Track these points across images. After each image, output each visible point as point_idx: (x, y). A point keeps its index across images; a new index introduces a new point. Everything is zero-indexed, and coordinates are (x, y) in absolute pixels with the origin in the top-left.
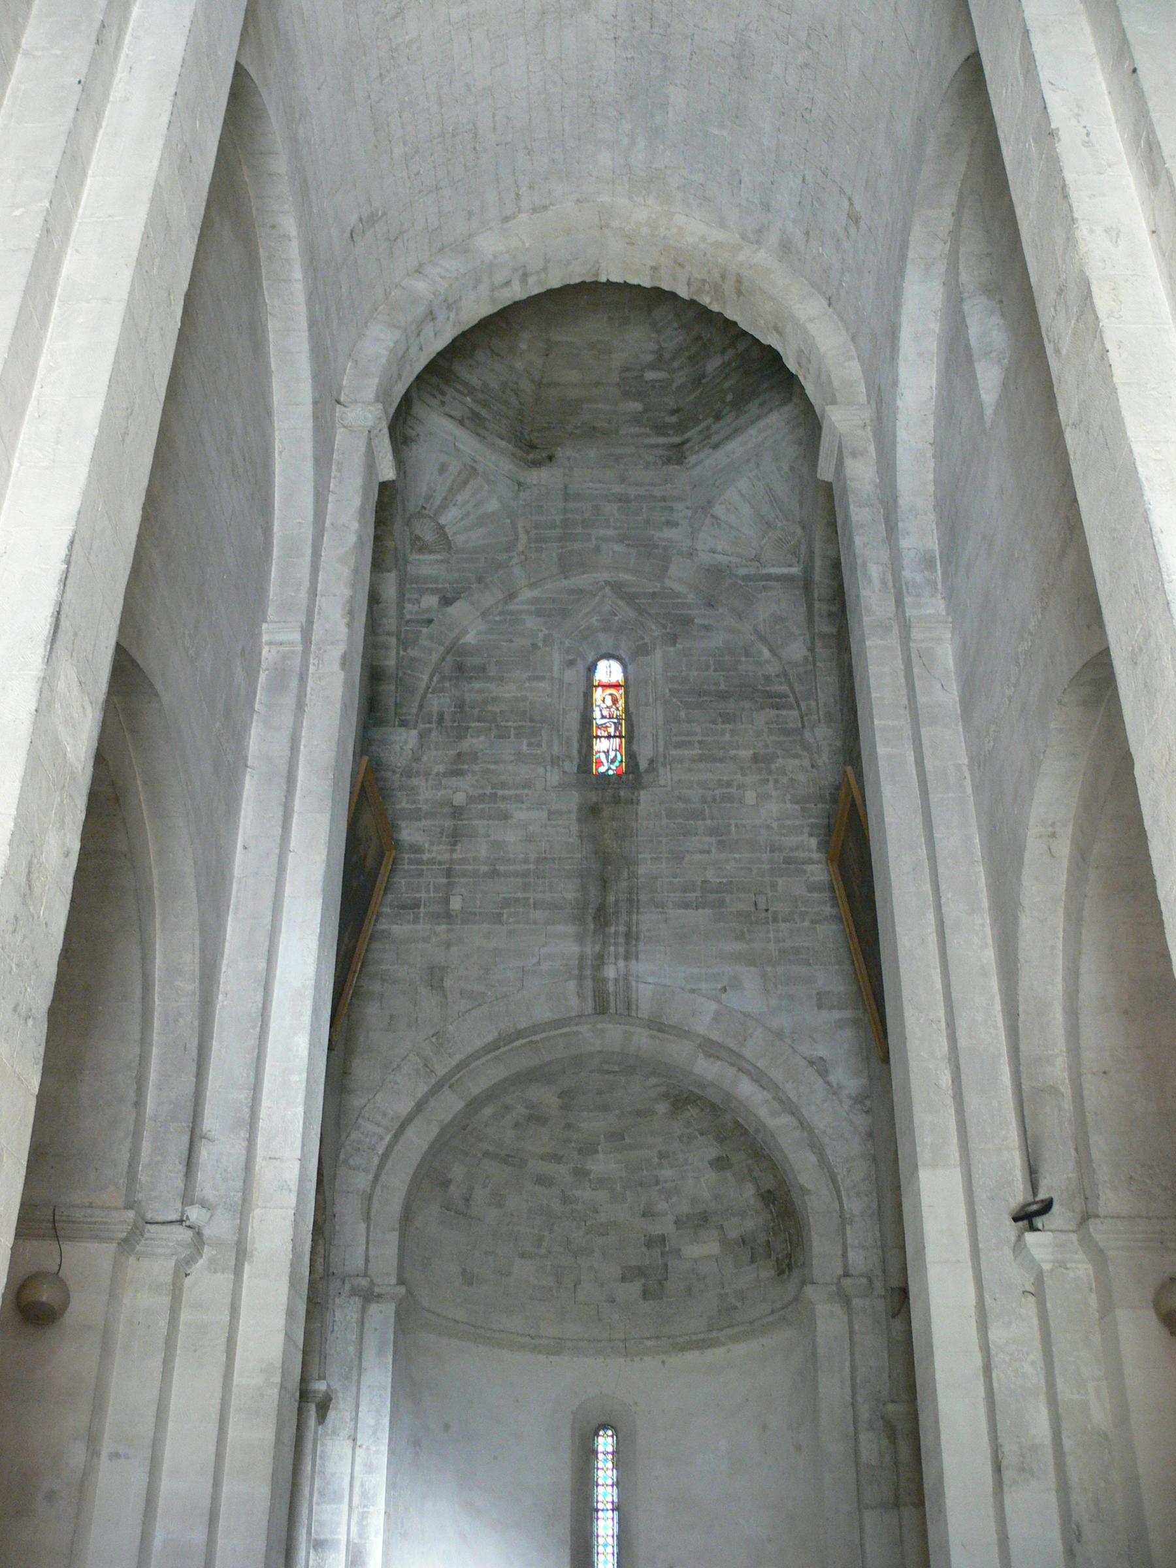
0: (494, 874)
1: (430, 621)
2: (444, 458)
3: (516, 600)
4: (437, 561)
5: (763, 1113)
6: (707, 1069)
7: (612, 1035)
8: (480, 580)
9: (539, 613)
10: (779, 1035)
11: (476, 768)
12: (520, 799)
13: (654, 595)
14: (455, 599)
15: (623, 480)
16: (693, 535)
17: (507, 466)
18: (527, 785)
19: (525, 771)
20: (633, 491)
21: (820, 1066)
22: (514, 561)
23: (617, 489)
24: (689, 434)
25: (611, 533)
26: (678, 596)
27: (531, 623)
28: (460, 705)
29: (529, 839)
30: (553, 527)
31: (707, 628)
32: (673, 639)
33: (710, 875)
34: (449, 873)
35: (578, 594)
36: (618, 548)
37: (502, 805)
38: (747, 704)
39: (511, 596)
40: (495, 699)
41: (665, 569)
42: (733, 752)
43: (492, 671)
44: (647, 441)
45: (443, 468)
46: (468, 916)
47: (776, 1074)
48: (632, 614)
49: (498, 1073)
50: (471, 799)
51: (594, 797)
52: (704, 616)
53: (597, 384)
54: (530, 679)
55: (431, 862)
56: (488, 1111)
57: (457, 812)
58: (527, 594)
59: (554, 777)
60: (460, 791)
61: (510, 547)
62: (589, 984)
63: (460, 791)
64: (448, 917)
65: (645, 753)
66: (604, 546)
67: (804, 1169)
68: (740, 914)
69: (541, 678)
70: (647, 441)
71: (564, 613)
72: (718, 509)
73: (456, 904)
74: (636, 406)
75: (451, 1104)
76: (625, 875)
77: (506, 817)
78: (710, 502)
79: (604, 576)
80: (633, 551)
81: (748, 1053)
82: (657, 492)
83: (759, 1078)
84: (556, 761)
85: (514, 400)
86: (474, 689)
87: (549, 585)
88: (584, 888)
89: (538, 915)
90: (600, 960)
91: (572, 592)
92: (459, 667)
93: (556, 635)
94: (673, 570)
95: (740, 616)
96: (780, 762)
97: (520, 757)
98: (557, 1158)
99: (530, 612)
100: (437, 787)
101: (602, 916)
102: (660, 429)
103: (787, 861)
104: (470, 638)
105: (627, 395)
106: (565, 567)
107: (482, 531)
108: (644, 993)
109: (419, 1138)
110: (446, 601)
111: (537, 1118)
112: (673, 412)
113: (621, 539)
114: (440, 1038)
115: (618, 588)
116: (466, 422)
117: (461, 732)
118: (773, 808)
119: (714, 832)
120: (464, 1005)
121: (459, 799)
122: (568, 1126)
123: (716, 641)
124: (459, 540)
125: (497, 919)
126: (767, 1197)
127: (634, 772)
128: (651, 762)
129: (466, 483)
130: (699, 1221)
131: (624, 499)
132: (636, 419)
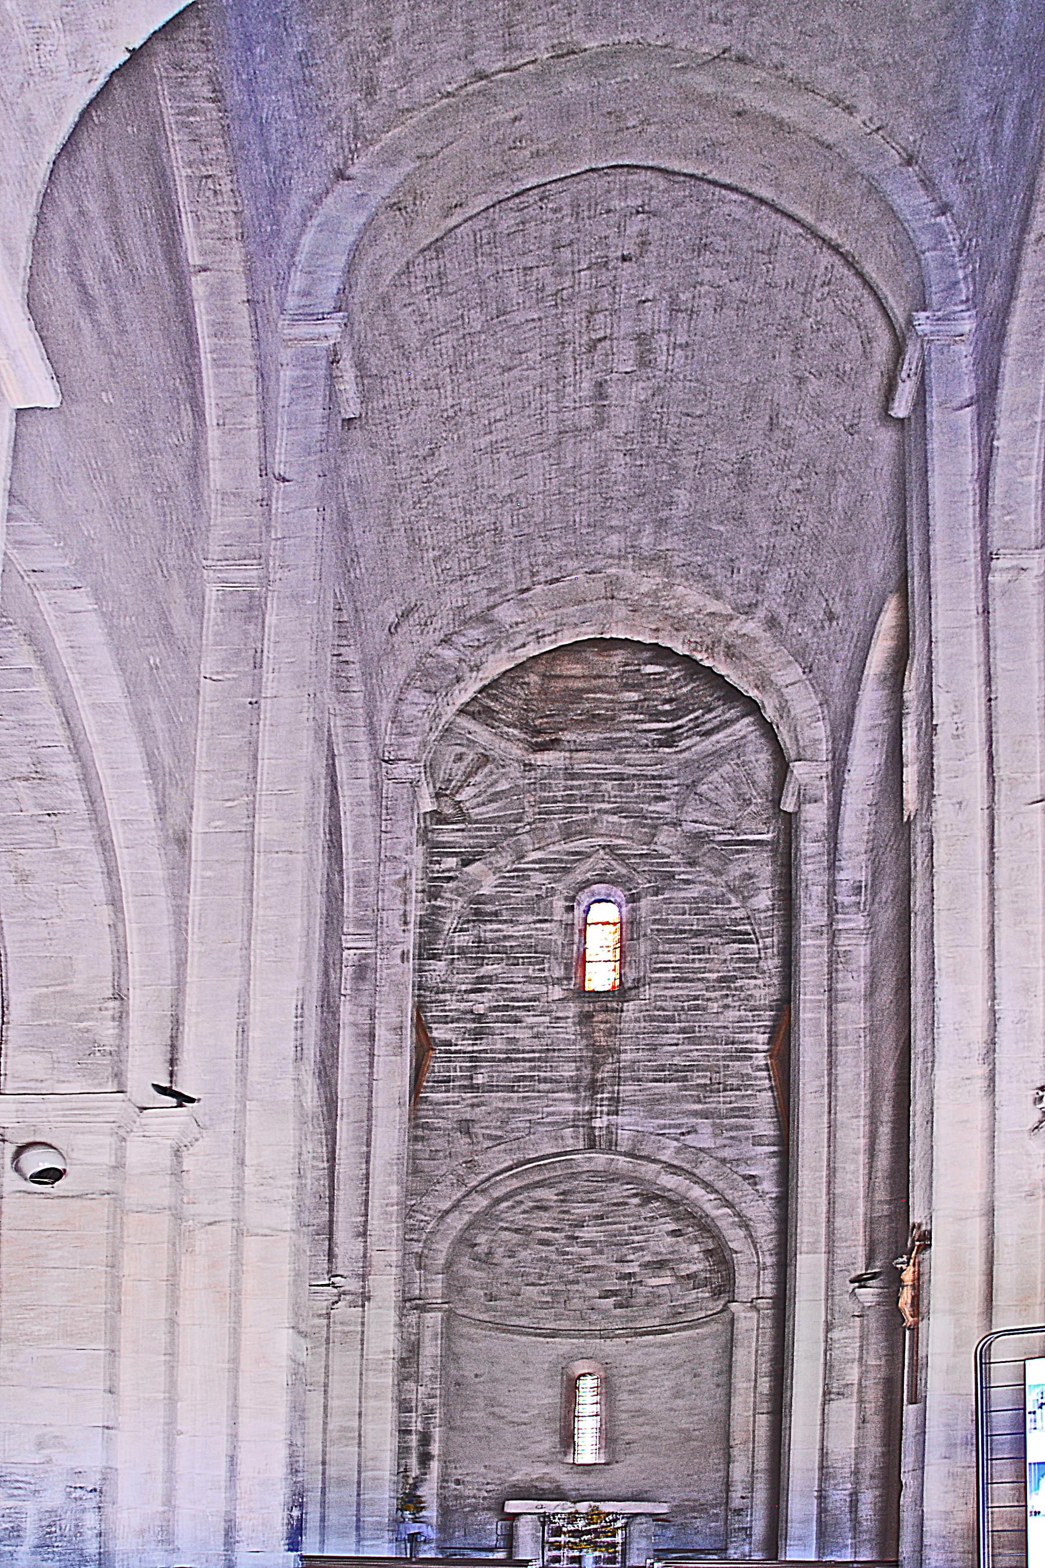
0: (509, 1060)
1: (449, 879)
3: (526, 860)
4: (458, 830)
5: (708, 1207)
6: (668, 1181)
7: (600, 1160)
10: (724, 1161)
12: (526, 1009)
17: (517, 751)
19: (533, 989)
21: (753, 1180)
27: (538, 878)
31: (687, 882)
35: (581, 856)
39: (521, 857)
44: (640, 727)
46: (491, 1088)
47: (720, 1185)
49: (515, 1184)
51: (588, 1008)
53: (600, 677)
56: (505, 1204)
57: (480, 1018)
59: (557, 993)
60: (482, 1003)
63: (482, 1003)
64: (474, 1088)
67: (735, 1239)
69: (546, 921)
70: (640, 727)
71: (566, 870)
72: (702, 788)
75: (483, 1202)
79: (601, 841)
83: (707, 1186)
84: (558, 981)
86: (488, 931)
89: (543, 1086)
94: (661, 838)
97: (529, 980)
101: (594, 1086)
102: (656, 716)
103: (742, 1050)
106: (567, 834)
107: (495, 805)
108: (624, 1138)
109: (457, 1222)
110: (466, 863)
112: (667, 701)
114: (471, 1165)
115: (611, 849)
117: (481, 962)
118: (732, 1014)
120: (488, 1143)
121: (480, 1009)
126: (709, 1253)
127: (621, 993)
130: (660, 1265)
132: (634, 708)
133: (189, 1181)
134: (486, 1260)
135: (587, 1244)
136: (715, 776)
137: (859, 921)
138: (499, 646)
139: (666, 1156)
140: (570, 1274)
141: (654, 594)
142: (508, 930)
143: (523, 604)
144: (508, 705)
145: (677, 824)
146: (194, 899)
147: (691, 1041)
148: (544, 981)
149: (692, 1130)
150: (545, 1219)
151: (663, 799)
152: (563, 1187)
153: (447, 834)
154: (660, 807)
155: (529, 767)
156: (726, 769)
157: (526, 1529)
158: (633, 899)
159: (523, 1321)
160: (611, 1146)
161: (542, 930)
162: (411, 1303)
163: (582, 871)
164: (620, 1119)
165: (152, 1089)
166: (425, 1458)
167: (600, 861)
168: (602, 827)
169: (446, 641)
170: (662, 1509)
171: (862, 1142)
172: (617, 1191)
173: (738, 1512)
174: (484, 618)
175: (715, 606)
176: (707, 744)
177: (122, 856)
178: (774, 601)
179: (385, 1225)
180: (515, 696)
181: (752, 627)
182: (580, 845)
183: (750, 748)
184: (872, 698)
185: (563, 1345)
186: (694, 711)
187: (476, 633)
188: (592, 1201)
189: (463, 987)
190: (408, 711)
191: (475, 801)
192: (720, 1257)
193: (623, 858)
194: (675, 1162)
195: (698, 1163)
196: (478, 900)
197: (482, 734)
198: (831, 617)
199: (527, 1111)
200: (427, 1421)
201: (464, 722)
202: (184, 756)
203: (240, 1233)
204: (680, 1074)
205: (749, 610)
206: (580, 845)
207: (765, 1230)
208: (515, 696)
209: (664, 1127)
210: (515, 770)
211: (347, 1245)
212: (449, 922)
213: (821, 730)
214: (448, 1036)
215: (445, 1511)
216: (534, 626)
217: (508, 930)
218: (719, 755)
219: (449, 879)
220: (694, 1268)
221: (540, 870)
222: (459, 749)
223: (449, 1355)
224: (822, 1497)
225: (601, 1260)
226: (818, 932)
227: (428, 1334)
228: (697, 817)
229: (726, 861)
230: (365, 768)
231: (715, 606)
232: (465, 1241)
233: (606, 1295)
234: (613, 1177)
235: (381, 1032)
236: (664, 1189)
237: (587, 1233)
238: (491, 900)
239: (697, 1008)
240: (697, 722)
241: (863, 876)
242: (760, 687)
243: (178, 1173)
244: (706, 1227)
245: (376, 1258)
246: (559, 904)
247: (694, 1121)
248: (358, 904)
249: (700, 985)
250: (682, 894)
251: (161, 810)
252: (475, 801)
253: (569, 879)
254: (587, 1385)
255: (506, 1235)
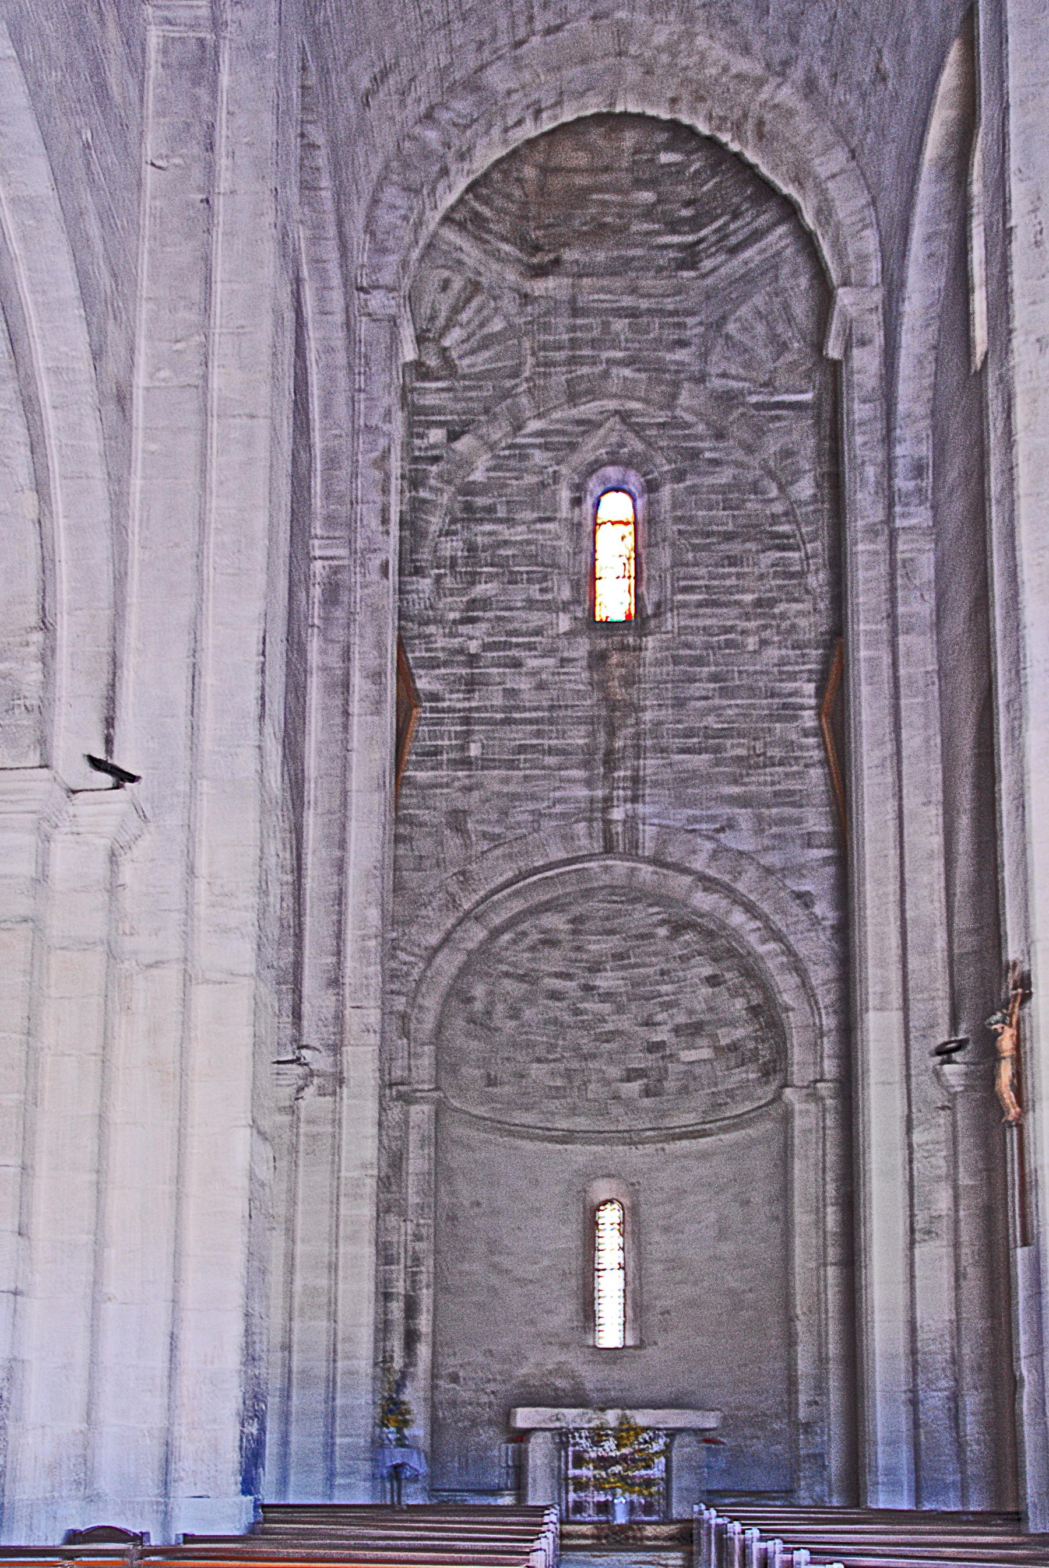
0: (507, 722)
2: (446, 274)
3: (524, 432)
4: (442, 390)
5: (753, 939)
6: (704, 901)
8: (486, 411)
9: (546, 447)
10: (769, 871)
11: (489, 614)
12: (531, 647)
13: (663, 425)
14: (463, 433)
15: (633, 291)
16: (704, 356)
17: (512, 276)
18: (538, 632)
19: (536, 619)
20: (644, 304)
21: (805, 899)
22: (521, 389)
23: (627, 301)
24: (703, 233)
25: (620, 355)
26: (688, 426)
27: (539, 457)
28: (471, 548)
29: (541, 686)
30: (560, 348)
31: (715, 462)
32: (679, 476)
33: (711, 721)
34: (466, 721)
35: (589, 425)
36: (627, 372)
37: (514, 653)
38: (751, 546)
39: (518, 428)
40: (506, 543)
41: (674, 396)
42: (737, 597)
43: (502, 513)
45: (445, 285)
46: (486, 763)
47: (766, 907)
48: (640, 447)
49: (518, 906)
50: (486, 647)
51: (602, 644)
52: (711, 450)
54: (541, 520)
55: (451, 710)
56: (507, 937)
57: (472, 660)
58: (534, 425)
59: (564, 623)
61: (515, 374)
62: (598, 825)
64: (466, 763)
65: (651, 598)
66: (614, 371)
68: (739, 759)
69: (548, 520)
71: (573, 447)
72: (731, 328)
73: (474, 750)
74: (647, 196)
75: (478, 934)
76: (631, 721)
77: (517, 664)
78: (724, 318)
79: (612, 405)
80: (644, 376)
81: (740, 887)
82: (669, 304)
83: (750, 908)
84: (565, 607)
85: (517, 193)
86: (483, 532)
87: (557, 415)
88: (592, 734)
89: (550, 760)
90: (608, 802)
91: (579, 422)
92: (468, 507)
93: (564, 470)
94: (684, 399)
95: (749, 449)
96: (781, 607)
97: (531, 604)
98: (568, 976)
99: (539, 446)
100: (452, 635)
101: (610, 761)
103: (785, 707)
104: (478, 476)
105: (639, 184)
106: (573, 398)
107: (487, 354)
109: (448, 963)
110: (453, 436)
111: (550, 942)
113: (628, 362)
114: (465, 877)
115: (624, 416)
116: (469, 226)
117: (473, 579)
118: (772, 654)
119: (714, 678)
120: (485, 845)
121: (473, 647)
122: (578, 949)
123: (725, 476)
124: (463, 364)
125: (512, 765)
128: (658, 605)
129: (468, 300)
130: (693, 1031)
131: (633, 313)
133: (128, 901)
134: (481, 1024)
135: (607, 996)
136: (743, 311)
137: (921, 516)
138: (490, 126)
139: (698, 864)
140: (586, 1043)
141: (671, 48)
142: (505, 532)
143: (518, 64)
144: (500, 211)
145: (701, 379)
146: (137, 483)
147: (724, 693)
148: (548, 606)
149: (730, 825)
150: (553, 960)
151: (682, 344)
152: (576, 910)
153: (432, 394)
154: (681, 355)
155: (526, 298)
156: (759, 300)
157: (538, 1451)
158: (651, 487)
159: (529, 1118)
160: (633, 851)
161: (543, 532)
162: (394, 1090)
163: (591, 449)
164: (641, 809)
165: (86, 766)
166: (411, 1338)
167: (612, 432)
168: (613, 385)
169: (429, 117)
170: (711, 1421)
171: (937, 842)
172: (642, 916)
173: (808, 1427)
174: (473, 85)
175: (742, 65)
176: (735, 265)
177: (50, 417)
178: (811, 59)
179: (362, 970)
180: (508, 197)
181: (786, 95)
182: (588, 409)
183: (785, 270)
184: (928, 189)
185: (580, 1154)
186: (717, 217)
187: (463, 105)
188: (611, 932)
189: (452, 616)
190: (386, 218)
191: (466, 346)
192: (767, 1015)
193: (638, 430)
194: (711, 872)
195: (737, 874)
196: (469, 489)
197: (471, 253)
198: (881, 76)
199: (533, 797)
200: (413, 1278)
201: (450, 235)
202: (122, 274)
203: (188, 979)
204: (710, 742)
205: (781, 69)
206: (588, 409)
207: (822, 975)
208: (508, 197)
209: (696, 820)
210: (509, 303)
211: (316, 999)
212: (435, 522)
213: (870, 242)
214: (436, 687)
215: (436, 1426)
216: (533, 97)
217: (505, 532)
218: (748, 279)
219: (436, 459)
220: (739, 1033)
221: (539, 446)
222: (446, 274)
223: (440, 1173)
224: (914, 1402)
225: (624, 1023)
226: (872, 532)
227: (414, 1137)
228: (725, 371)
229: (760, 432)
230: (336, 299)
231: (742, 65)
232: (457, 994)
233: (631, 1075)
234: (635, 895)
235: (357, 680)
236: (696, 912)
237: (604, 981)
238: (484, 489)
239: (729, 644)
240: (722, 234)
241: (925, 450)
242: (797, 180)
243: (113, 888)
244: (751, 972)
245: (353, 1019)
246: (565, 495)
247: (727, 811)
248: (328, 495)
249: (735, 611)
250: (709, 480)
251: (97, 355)
252: (466, 346)
253: (577, 459)
254: (610, 1216)
255: (508, 985)
